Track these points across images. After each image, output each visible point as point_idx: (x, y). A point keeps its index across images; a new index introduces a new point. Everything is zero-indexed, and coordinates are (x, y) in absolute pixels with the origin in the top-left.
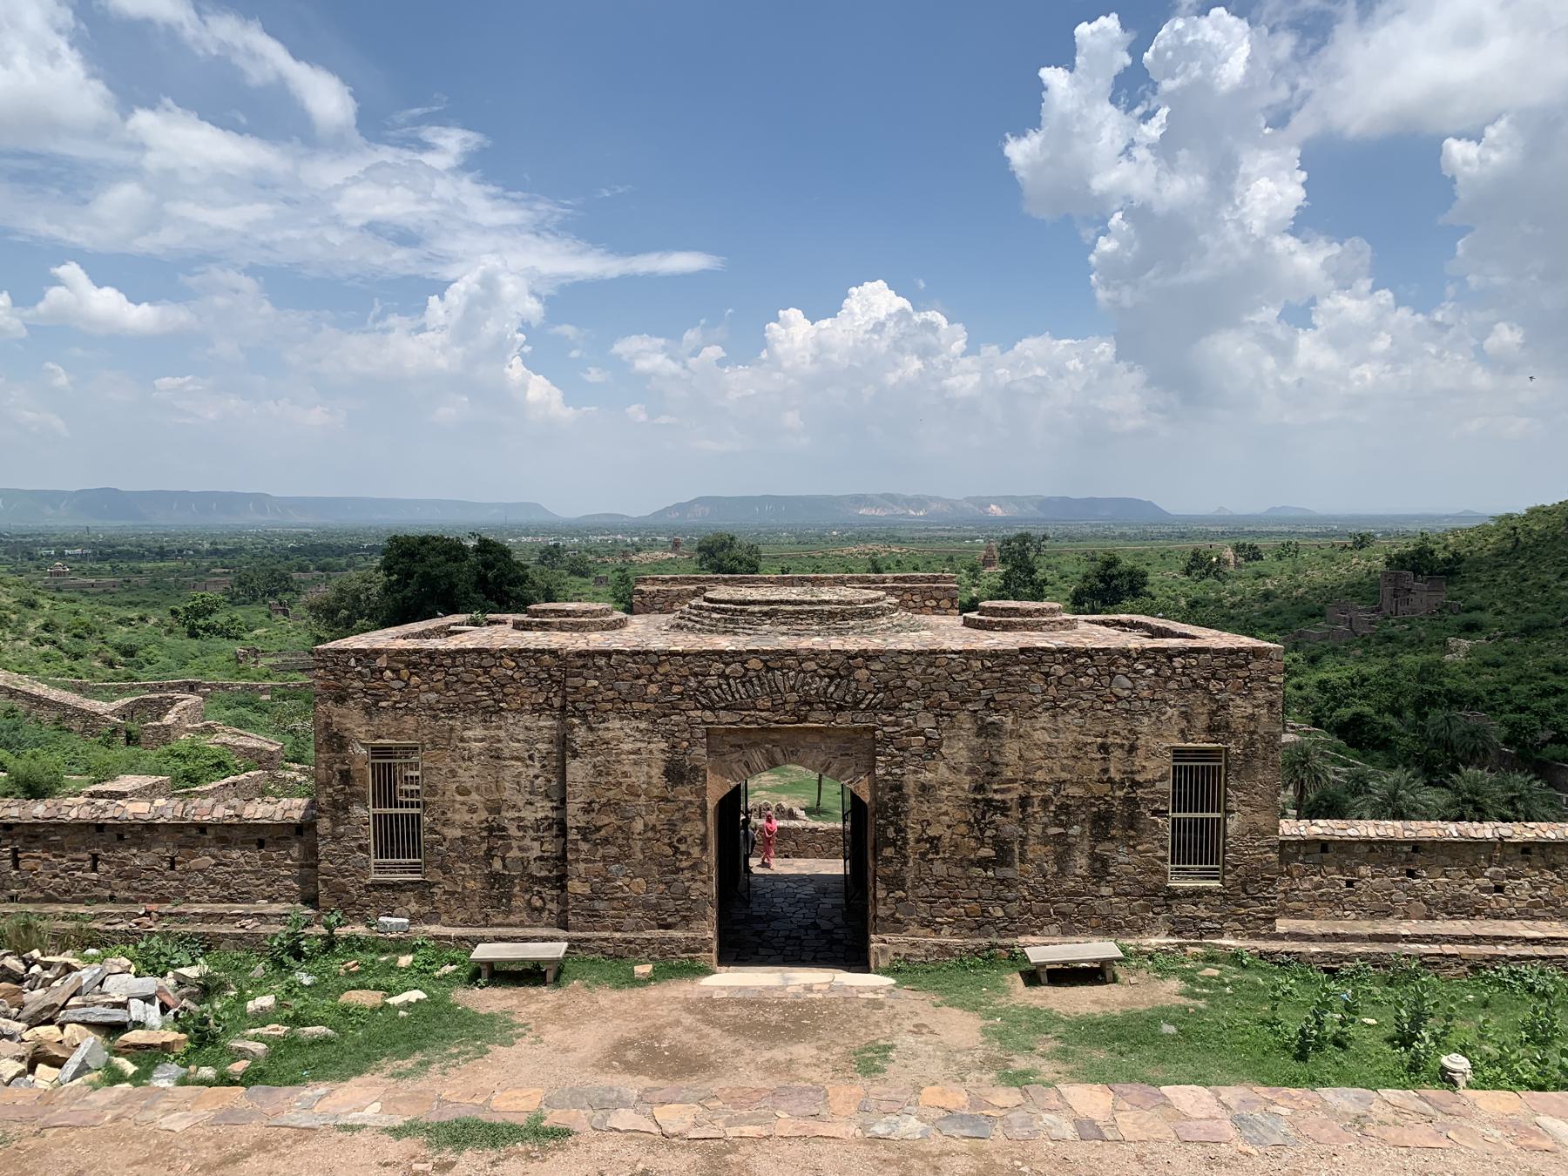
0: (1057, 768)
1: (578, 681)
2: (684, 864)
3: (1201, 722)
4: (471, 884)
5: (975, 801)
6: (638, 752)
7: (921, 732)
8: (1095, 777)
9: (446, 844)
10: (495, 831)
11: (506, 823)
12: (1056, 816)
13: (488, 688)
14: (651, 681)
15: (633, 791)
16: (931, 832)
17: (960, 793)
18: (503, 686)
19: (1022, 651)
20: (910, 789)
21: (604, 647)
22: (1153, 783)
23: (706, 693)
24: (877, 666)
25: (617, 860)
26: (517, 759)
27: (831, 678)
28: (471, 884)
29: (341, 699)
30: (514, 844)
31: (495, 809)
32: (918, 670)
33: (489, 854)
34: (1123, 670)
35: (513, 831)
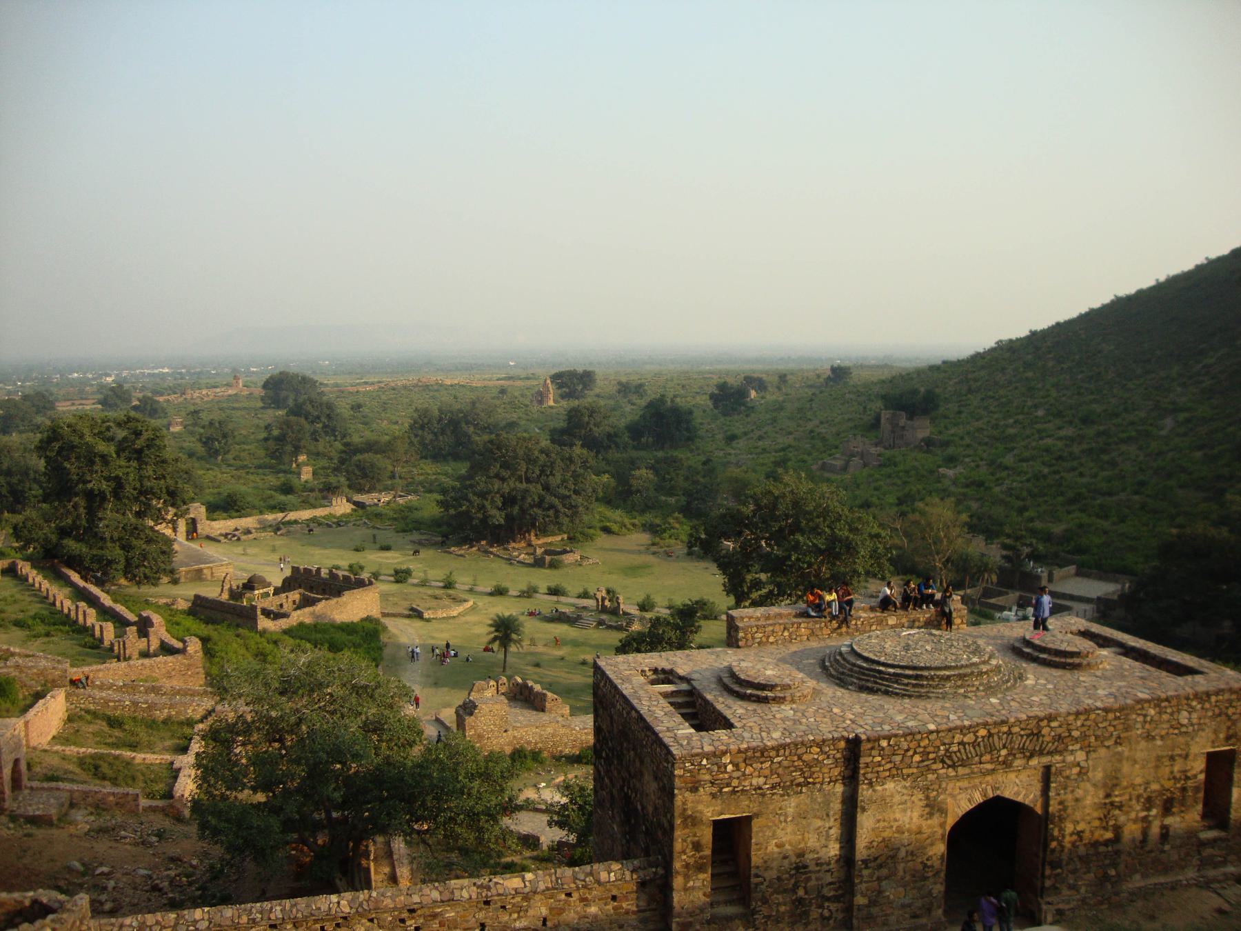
1: (869, 760)
2: (930, 874)
6: (905, 803)
9: (766, 884)
14: (915, 753)
16: (1079, 828)
17: (1096, 800)
18: (811, 767)
20: (1070, 803)
22: (1195, 776)
23: (950, 758)
24: (1054, 724)
25: (886, 878)
27: (1028, 736)
28: (782, 909)
29: (694, 789)
30: (813, 876)
32: (1079, 723)
35: (812, 867)
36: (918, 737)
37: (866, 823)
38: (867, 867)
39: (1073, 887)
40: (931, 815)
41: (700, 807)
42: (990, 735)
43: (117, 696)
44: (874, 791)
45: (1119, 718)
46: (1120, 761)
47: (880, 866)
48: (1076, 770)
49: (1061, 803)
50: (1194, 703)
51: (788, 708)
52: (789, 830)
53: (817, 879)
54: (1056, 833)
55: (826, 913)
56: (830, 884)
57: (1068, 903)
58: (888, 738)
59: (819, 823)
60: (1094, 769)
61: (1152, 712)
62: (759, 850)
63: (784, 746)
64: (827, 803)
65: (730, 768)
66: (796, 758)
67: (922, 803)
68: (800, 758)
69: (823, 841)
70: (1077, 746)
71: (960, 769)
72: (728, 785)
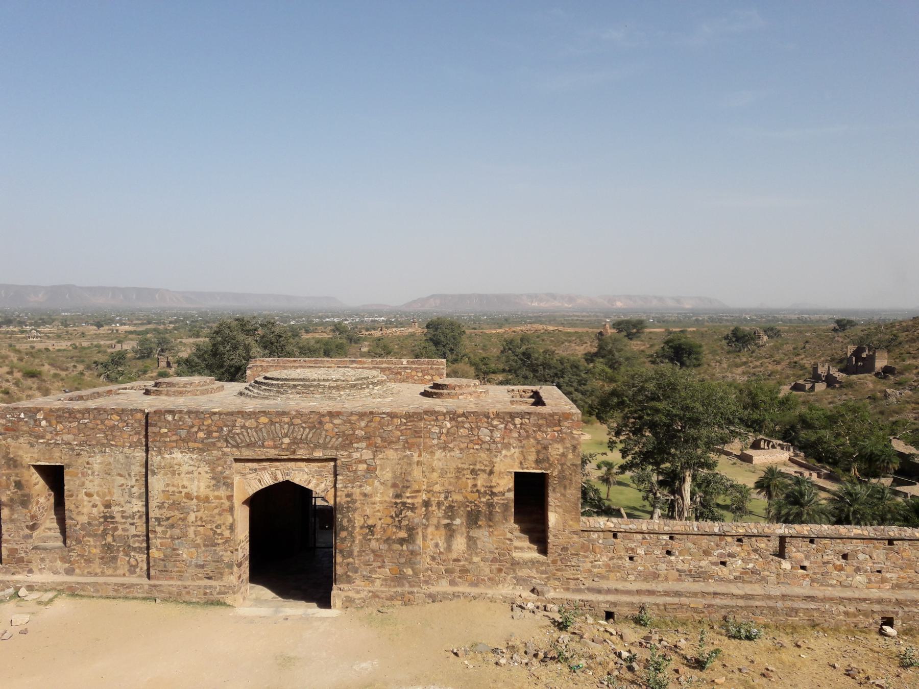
0: (446, 485)
2: (220, 541)
3: (532, 457)
4: (94, 551)
5: (396, 503)
6: (192, 473)
7: (365, 462)
8: (469, 489)
9: (79, 527)
10: (108, 518)
11: (115, 514)
12: (446, 513)
13: (104, 433)
14: (199, 430)
15: (189, 496)
16: (370, 522)
17: (387, 499)
19: (426, 412)
21: (171, 407)
24: (336, 421)
26: (121, 475)
30: (120, 527)
31: (108, 506)
32: (363, 424)
33: (105, 534)
34: (485, 425)
35: (118, 518)
36: (202, 416)
37: (157, 484)
38: (159, 525)
39: (368, 579)
40: (216, 487)
41: (21, 453)
42: (272, 423)
44: (163, 458)
45: (405, 424)
46: (410, 464)
47: (172, 526)
48: (362, 467)
49: (348, 496)
50: (495, 423)
52: (96, 482)
53: (124, 530)
54: (345, 523)
55: (133, 562)
56: (136, 536)
57: (358, 592)
59: (121, 480)
60: (382, 469)
61: (449, 425)
62: (72, 496)
64: (128, 465)
65: (44, 423)
66: (99, 422)
67: (208, 476)
68: (102, 423)
69: (127, 498)
70: (364, 445)
71: (243, 450)
72: (43, 437)
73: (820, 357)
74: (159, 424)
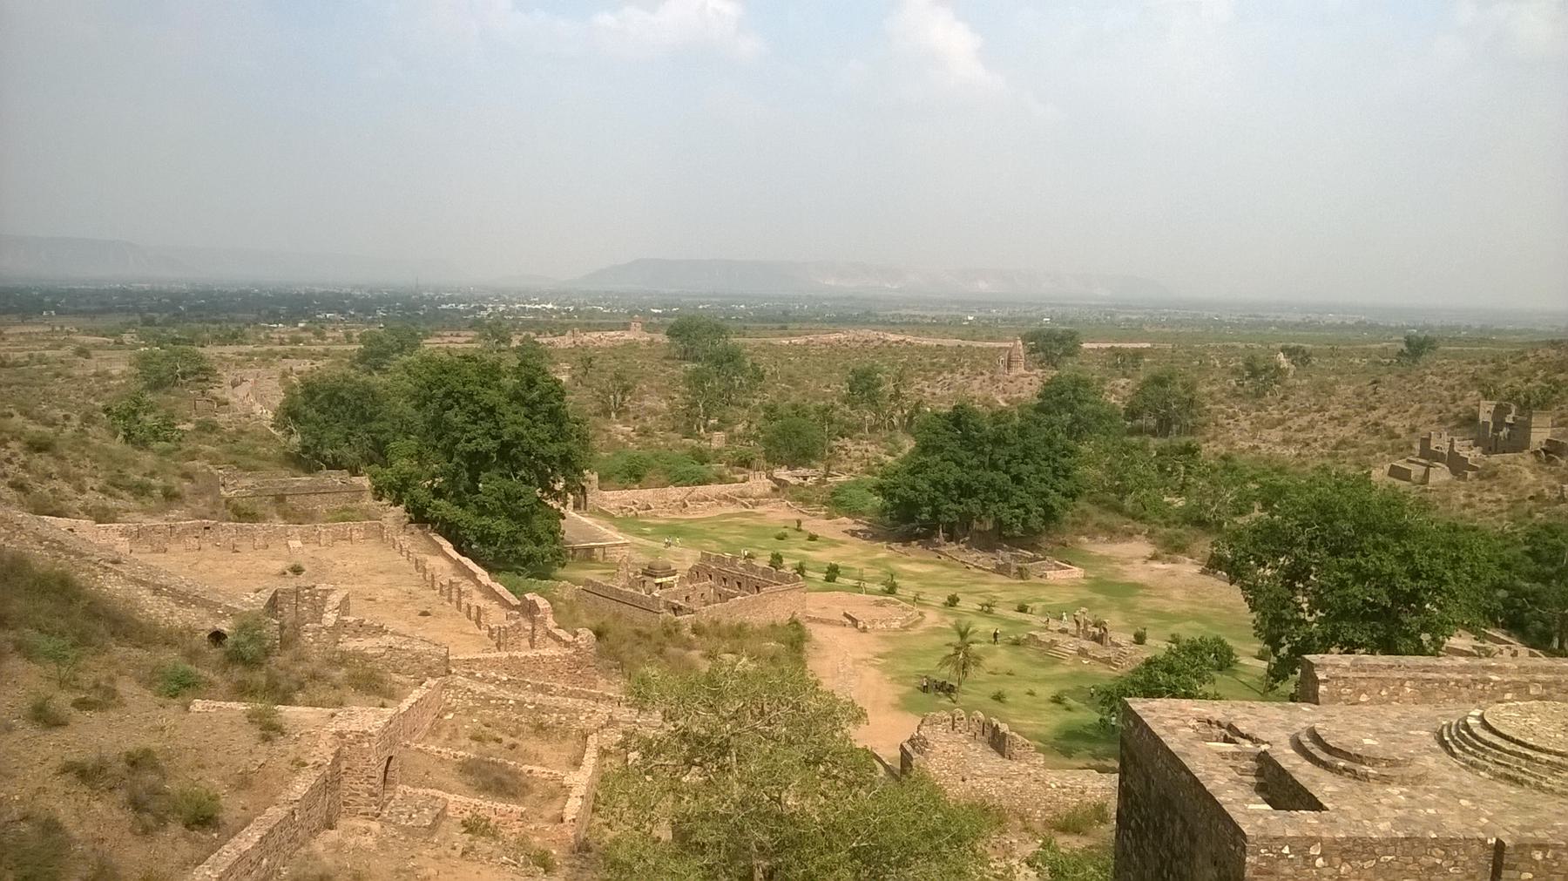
43: (502, 693)
51: (1396, 791)
58: (1542, 846)
63: (1394, 841)
65: (1320, 862)
73: (1417, 414)
74: (1521, 865)
